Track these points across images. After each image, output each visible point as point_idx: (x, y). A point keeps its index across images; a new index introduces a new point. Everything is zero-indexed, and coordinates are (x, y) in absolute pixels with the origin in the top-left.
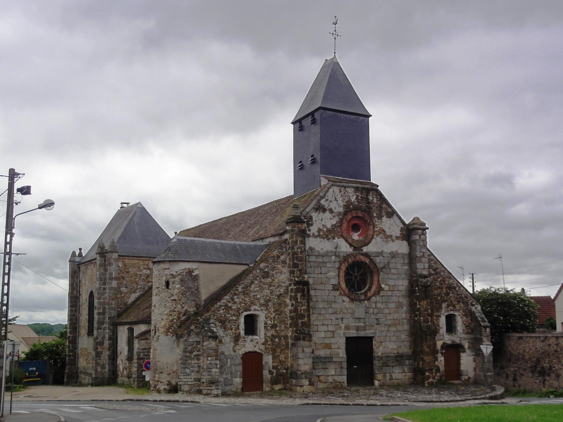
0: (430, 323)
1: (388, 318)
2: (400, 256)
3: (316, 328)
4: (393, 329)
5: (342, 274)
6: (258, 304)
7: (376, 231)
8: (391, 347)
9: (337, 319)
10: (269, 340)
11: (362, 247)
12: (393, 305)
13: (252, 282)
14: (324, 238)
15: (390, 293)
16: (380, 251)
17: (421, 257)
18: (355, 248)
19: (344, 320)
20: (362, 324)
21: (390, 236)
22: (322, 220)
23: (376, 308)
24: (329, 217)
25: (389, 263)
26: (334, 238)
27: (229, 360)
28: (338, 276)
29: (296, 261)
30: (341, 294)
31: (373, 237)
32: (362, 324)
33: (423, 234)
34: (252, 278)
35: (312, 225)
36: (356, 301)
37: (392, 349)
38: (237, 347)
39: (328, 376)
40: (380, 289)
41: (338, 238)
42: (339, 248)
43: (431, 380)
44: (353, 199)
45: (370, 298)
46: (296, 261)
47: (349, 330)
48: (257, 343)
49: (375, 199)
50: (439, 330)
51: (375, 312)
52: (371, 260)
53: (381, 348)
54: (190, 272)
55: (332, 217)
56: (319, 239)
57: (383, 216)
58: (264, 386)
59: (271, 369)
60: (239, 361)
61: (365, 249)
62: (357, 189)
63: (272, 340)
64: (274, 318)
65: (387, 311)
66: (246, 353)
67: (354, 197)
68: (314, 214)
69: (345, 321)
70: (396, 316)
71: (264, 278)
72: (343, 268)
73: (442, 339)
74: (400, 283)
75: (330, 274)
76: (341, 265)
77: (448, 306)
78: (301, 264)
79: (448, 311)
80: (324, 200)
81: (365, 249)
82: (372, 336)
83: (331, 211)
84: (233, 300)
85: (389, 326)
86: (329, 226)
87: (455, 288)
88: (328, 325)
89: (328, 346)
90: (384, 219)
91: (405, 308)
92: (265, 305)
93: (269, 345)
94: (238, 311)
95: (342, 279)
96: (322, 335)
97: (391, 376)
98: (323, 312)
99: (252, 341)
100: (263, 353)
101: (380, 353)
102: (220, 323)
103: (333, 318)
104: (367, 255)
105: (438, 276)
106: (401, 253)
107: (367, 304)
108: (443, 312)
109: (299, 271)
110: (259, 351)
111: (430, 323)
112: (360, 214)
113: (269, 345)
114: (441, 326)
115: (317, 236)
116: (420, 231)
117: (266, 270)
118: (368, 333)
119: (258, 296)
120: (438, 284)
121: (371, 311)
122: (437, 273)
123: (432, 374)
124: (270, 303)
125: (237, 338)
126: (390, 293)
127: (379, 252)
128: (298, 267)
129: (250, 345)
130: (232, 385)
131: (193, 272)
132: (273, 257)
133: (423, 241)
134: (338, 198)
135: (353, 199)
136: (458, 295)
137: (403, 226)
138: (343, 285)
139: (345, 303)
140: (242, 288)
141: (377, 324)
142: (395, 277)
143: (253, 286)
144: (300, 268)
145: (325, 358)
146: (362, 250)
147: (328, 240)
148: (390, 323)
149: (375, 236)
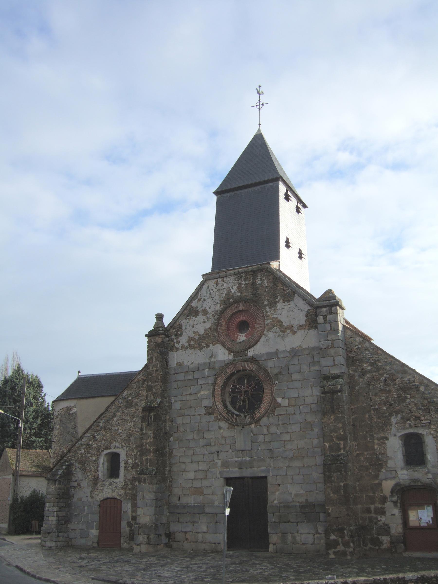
0: (342, 451)
1: (289, 447)
2: (307, 352)
3: (183, 466)
4: (297, 464)
5: (218, 391)
6: (119, 440)
7: (268, 324)
8: (294, 492)
9: (212, 453)
10: (129, 483)
11: (246, 349)
12: (295, 428)
13: (114, 415)
14: (195, 349)
15: (291, 410)
16: (273, 350)
17: (327, 348)
18: (236, 354)
19: (220, 454)
20: (248, 459)
21: (290, 327)
22: (193, 327)
23: (269, 433)
24: (202, 321)
25: (287, 366)
26: (208, 346)
27: (86, 508)
28: (213, 393)
29: (150, 383)
30: (216, 417)
31: (262, 334)
32: (248, 459)
33: (331, 313)
34: (114, 410)
35: (181, 335)
36: (238, 426)
37: (296, 495)
38: (95, 492)
39: (199, 533)
40: (275, 405)
41: (214, 345)
42: (215, 358)
43: (341, 548)
44: (234, 290)
45: (260, 419)
46: (150, 383)
47: (227, 467)
48: (116, 487)
49: (265, 282)
50: (386, 462)
51: (267, 440)
52: (260, 366)
53: (277, 493)
54: (68, 409)
55: (206, 320)
56: (189, 351)
57: (278, 302)
58: (122, 541)
59: (130, 520)
60: (96, 508)
61: (250, 353)
62: (238, 275)
63: (132, 484)
64: (135, 455)
65: (287, 437)
66: (104, 500)
67: (235, 288)
68: (184, 321)
69: (222, 455)
70: (301, 444)
71: (126, 407)
72: (220, 381)
73: (394, 478)
74: (308, 392)
75: (202, 393)
76: (216, 379)
77: (404, 419)
78: (156, 386)
79: (404, 428)
80: (196, 300)
81: (250, 353)
82: (263, 475)
83: (205, 312)
84: (94, 437)
85: (291, 459)
86: (202, 332)
87: (417, 388)
88: (198, 462)
89: (199, 491)
90: (280, 305)
91: (316, 430)
92: (127, 441)
93: (130, 489)
94: (98, 450)
95: (218, 398)
96: (191, 475)
97: (294, 538)
98: (192, 444)
99: (110, 485)
100: (122, 499)
101: (276, 502)
102: (79, 464)
103: (206, 452)
104: (254, 360)
105: (381, 372)
106: (308, 349)
107: (255, 430)
108: (393, 430)
109: (153, 395)
110: (118, 497)
111: (342, 451)
112: (242, 307)
113: (130, 489)
114: (390, 454)
115: (187, 348)
116: (324, 310)
117: (130, 398)
118: (257, 471)
119: (120, 431)
120: (381, 385)
121: (261, 438)
122: (378, 369)
123: (342, 537)
124: (132, 438)
125: (95, 481)
126: (291, 410)
127: (270, 353)
128: (152, 390)
129: (111, 489)
130: (88, 537)
131: (70, 410)
132: (138, 382)
133: (330, 323)
134: (213, 294)
135: (234, 290)
136: (425, 398)
137: (309, 308)
138: (220, 406)
139: (222, 431)
140: (104, 422)
141: (271, 458)
142: (298, 384)
143: (115, 419)
144: (154, 391)
145: (194, 507)
146: (247, 355)
147: (200, 349)
148: (291, 455)
149: (265, 332)
